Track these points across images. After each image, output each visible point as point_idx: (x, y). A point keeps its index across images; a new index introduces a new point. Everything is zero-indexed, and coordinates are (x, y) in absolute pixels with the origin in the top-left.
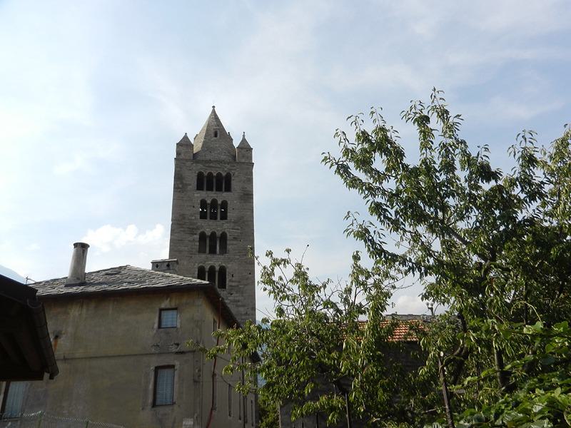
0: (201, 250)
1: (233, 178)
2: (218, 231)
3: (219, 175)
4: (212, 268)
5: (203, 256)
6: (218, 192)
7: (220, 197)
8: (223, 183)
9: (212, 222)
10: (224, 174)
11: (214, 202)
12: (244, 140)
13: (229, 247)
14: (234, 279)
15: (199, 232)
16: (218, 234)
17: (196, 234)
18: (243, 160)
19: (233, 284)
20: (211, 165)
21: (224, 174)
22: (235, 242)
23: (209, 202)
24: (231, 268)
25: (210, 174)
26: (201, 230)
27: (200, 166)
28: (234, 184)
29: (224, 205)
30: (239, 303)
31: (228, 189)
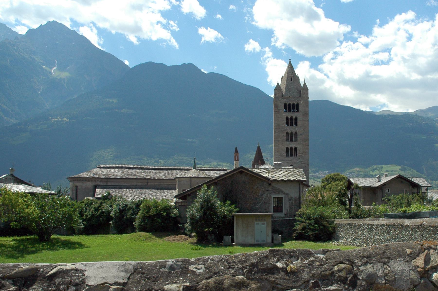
0: (287, 140)
1: (300, 105)
2: (294, 131)
3: (293, 104)
4: (291, 148)
5: (288, 143)
6: (293, 113)
7: (294, 115)
8: (294, 108)
9: (291, 127)
10: (296, 104)
11: (292, 118)
12: (305, 84)
13: (298, 138)
14: (300, 152)
15: (286, 132)
16: (294, 133)
17: (284, 133)
18: (304, 96)
19: (300, 154)
20: (290, 99)
21: (296, 104)
22: (300, 136)
23: (289, 118)
24: (299, 147)
25: (290, 104)
26: (287, 131)
27: (285, 100)
28: (300, 108)
29: (296, 119)
30: (303, 163)
31: (298, 111)
